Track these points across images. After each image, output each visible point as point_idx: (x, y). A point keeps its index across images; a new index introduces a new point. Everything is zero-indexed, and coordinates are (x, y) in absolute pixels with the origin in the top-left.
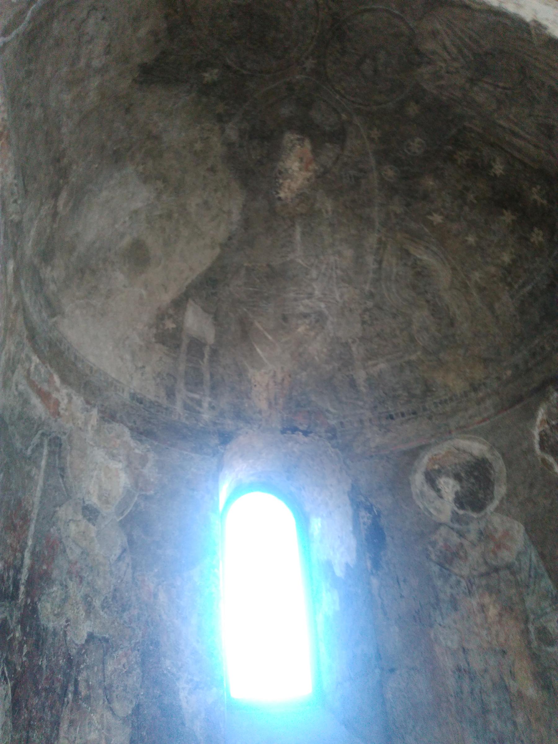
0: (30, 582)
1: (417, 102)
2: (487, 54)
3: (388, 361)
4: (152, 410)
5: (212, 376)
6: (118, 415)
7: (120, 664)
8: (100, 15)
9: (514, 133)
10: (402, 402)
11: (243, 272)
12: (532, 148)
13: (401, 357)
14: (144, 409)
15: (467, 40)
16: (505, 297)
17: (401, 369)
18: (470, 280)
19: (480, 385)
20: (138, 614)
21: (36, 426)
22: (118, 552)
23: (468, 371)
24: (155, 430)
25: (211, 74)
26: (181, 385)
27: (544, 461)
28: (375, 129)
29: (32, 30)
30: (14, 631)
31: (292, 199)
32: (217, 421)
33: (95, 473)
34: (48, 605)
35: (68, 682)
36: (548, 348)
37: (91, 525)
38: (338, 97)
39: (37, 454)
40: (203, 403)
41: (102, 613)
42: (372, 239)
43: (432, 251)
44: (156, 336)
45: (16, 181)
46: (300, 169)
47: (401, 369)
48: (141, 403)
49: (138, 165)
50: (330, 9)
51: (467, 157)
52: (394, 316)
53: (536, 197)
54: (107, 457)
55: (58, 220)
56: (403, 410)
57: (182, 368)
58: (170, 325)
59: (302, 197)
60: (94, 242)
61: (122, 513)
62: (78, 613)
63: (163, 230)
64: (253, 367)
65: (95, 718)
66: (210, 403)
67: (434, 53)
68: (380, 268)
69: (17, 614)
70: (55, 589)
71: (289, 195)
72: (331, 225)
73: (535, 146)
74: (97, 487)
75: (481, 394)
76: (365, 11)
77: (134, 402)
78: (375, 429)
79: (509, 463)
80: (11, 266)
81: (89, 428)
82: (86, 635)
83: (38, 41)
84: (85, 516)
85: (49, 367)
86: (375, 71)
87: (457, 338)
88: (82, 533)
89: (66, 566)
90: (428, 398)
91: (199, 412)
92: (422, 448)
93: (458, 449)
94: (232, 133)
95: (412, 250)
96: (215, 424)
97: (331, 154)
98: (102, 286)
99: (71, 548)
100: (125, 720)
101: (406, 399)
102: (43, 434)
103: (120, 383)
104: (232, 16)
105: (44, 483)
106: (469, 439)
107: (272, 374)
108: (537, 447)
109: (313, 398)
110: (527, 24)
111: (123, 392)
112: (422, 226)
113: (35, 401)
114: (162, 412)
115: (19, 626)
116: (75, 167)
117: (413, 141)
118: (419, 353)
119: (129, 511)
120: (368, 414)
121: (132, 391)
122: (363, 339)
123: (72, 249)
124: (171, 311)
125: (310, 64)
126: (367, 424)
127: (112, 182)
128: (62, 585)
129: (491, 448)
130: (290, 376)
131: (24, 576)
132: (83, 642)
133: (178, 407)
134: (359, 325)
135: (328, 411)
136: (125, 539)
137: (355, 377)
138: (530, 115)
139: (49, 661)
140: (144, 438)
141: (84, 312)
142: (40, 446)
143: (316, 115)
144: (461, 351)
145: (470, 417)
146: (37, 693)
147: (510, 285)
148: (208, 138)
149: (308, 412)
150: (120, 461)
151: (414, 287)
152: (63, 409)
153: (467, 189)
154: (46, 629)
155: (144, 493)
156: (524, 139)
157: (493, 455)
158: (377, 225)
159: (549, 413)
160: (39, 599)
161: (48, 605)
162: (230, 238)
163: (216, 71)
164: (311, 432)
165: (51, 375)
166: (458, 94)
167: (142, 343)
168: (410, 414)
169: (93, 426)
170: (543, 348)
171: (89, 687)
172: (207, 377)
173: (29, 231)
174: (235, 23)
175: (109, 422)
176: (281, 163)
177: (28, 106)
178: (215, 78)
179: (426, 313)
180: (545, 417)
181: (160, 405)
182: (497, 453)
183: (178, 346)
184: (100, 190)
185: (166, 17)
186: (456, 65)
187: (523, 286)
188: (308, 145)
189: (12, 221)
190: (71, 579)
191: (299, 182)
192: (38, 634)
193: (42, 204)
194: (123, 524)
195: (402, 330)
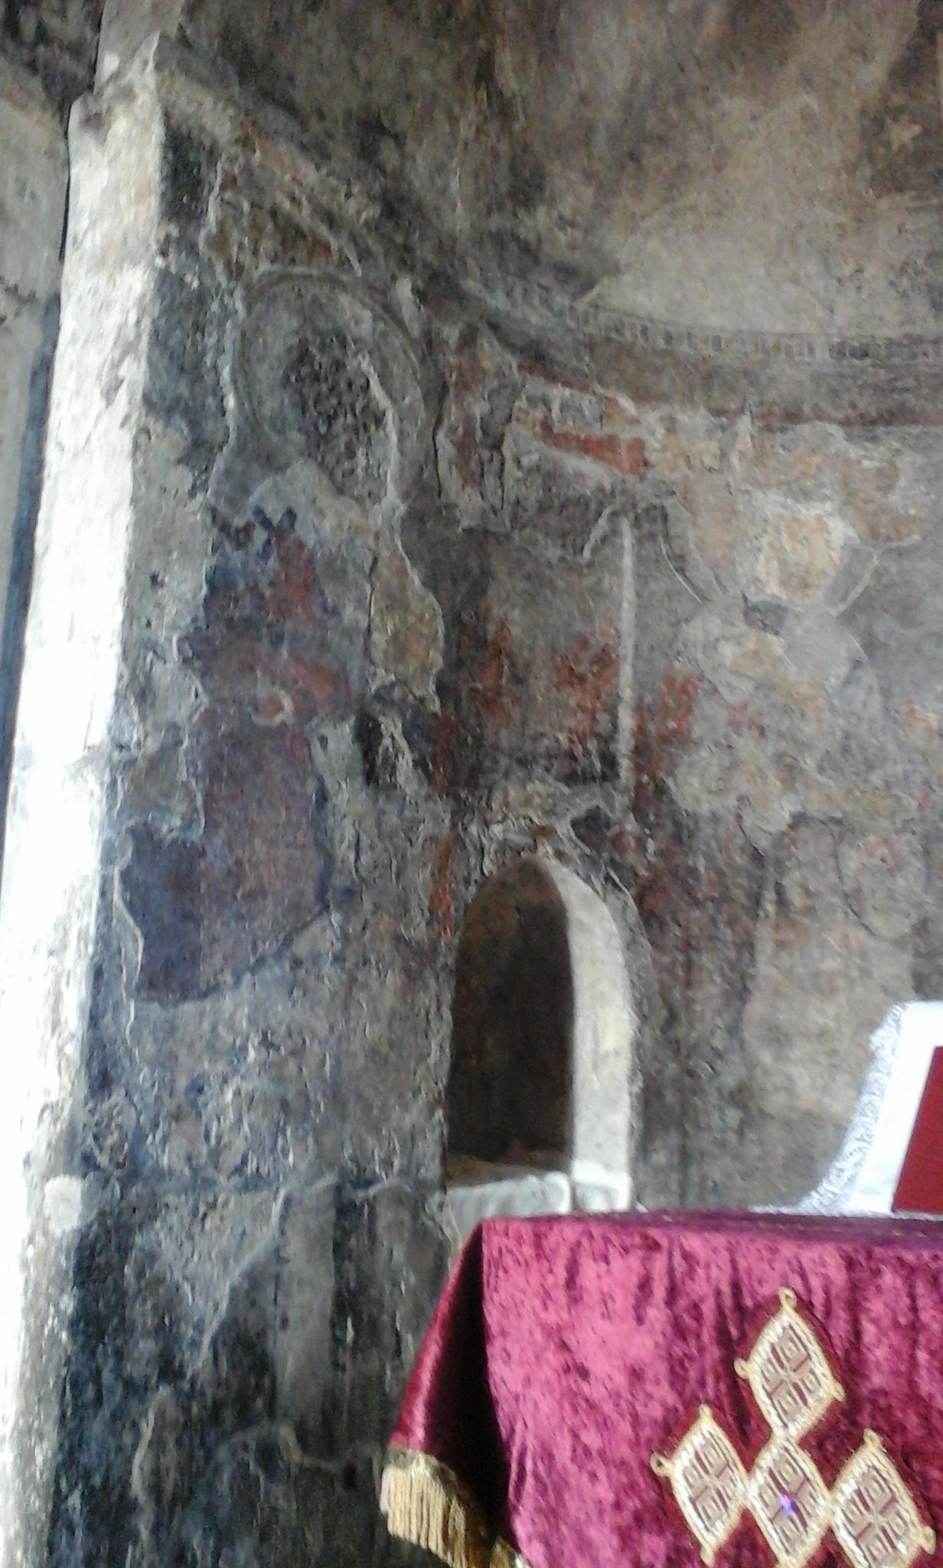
0: (640, 751)
6: (806, 409)
21: (593, 506)
22: (843, 670)
30: (620, 822)
33: (764, 541)
34: (695, 782)
35: (761, 887)
37: (771, 637)
39: (608, 551)
44: (873, 182)
45: (324, 172)
48: (865, 354)
54: (789, 501)
60: (635, 82)
61: (844, 599)
65: (833, 939)
69: (621, 801)
70: (704, 753)
74: (775, 564)
77: (845, 362)
84: (751, 623)
85: (600, 390)
89: (723, 716)
99: (729, 685)
100: (899, 943)
102: (614, 514)
105: (638, 595)
111: (811, 350)
113: (574, 463)
115: (631, 815)
121: (836, 340)
128: (717, 744)
131: (624, 745)
132: (784, 827)
136: (856, 644)
139: (710, 859)
140: (880, 430)
141: (670, 233)
142: (615, 532)
146: (697, 903)
150: (826, 498)
154: (694, 817)
155: (894, 545)
160: (670, 773)
161: (695, 782)
165: (612, 402)
167: (843, 219)
169: (742, 454)
171: (808, 893)
175: (783, 430)
181: (919, 340)
190: (738, 733)
192: (677, 824)
194: (848, 618)
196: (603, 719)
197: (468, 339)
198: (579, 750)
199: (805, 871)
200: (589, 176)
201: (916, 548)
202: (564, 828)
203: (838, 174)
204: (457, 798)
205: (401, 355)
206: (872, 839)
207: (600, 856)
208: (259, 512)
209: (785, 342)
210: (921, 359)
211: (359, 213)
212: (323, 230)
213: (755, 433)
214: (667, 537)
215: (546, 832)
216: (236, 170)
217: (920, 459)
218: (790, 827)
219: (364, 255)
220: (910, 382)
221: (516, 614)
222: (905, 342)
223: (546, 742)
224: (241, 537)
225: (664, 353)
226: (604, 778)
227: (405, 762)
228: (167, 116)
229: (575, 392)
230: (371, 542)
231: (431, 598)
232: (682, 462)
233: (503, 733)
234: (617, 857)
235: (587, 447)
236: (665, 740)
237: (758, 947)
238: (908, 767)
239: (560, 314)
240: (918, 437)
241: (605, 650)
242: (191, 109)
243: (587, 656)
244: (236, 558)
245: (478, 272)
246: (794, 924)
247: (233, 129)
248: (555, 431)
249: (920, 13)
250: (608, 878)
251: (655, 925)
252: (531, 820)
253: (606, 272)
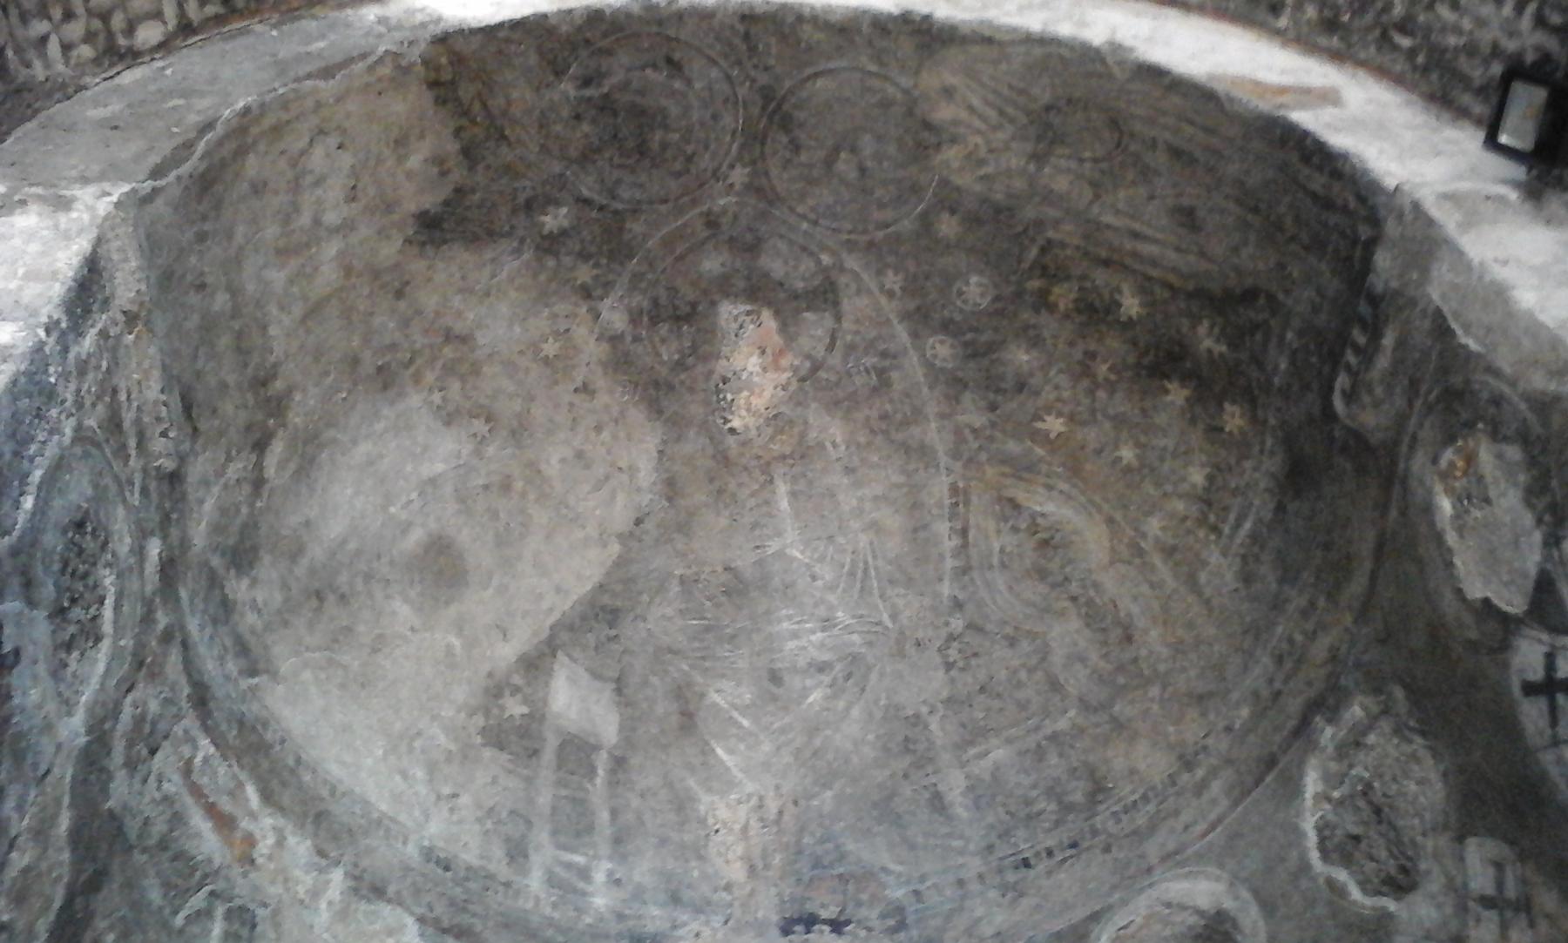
1: (953, 212)
2: (1048, 108)
3: (1009, 741)
4: (473, 885)
5: (614, 813)
8: (333, 141)
9: (1136, 235)
10: (1047, 825)
11: (675, 588)
12: (1172, 255)
13: (1037, 728)
15: (1006, 91)
16: (1214, 557)
17: (1039, 754)
18: (1144, 536)
19: (1197, 754)
21: (198, 874)
23: (1171, 729)
24: (479, 928)
25: (556, 217)
26: (542, 836)
27: (1331, 883)
28: (890, 273)
29: (208, 170)
31: (758, 428)
32: (627, 912)
36: (1299, 638)
38: (805, 226)
39: (195, 929)
42: (938, 488)
43: (1061, 492)
44: (483, 731)
45: (163, 397)
46: (765, 369)
47: (1039, 754)
48: (447, 869)
49: (431, 390)
50: (753, 81)
51: (1073, 296)
52: (1012, 642)
53: (1208, 343)
55: (265, 495)
56: (1050, 843)
57: (544, 799)
58: (515, 708)
59: (776, 421)
60: (344, 542)
63: (495, 515)
64: (709, 790)
66: (610, 874)
67: (956, 123)
68: (965, 545)
71: (751, 421)
72: (849, 470)
73: (1178, 249)
75: (1200, 773)
76: (816, 75)
78: (993, 894)
79: (1268, 907)
80: (154, 548)
81: (323, 906)
83: (219, 188)
85: (236, 768)
86: (863, 170)
87: (1144, 666)
90: (1101, 808)
91: (584, 894)
92: (1095, 917)
93: (1168, 905)
94: (615, 316)
95: (1021, 496)
96: (621, 917)
97: (819, 332)
98: (361, 628)
101: (1054, 817)
102: (212, 894)
104: (578, 117)
106: (1187, 876)
107: (754, 801)
108: (1314, 856)
109: (850, 846)
110: (1097, 51)
111: (405, 843)
112: (1029, 443)
113: (199, 822)
114: (496, 893)
116: (298, 397)
117: (967, 283)
118: (1072, 713)
120: (975, 865)
121: (426, 843)
122: (949, 701)
123: (296, 554)
124: (517, 680)
125: (739, 176)
126: (974, 887)
127: (379, 426)
129: (1232, 884)
130: (796, 803)
133: (535, 882)
134: (941, 673)
135: (884, 869)
137: (941, 788)
138: (1151, 198)
141: (323, 676)
142: (204, 914)
143: (774, 264)
144: (1154, 691)
145: (1186, 828)
147: (1215, 529)
148: (567, 330)
149: (840, 876)
151: (1042, 574)
152: (262, 855)
153: (1092, 356)
156: (1156, 241)
157: (1236, 898)
158: (944, 460)
159: (1327, 778)
162: (638, 522)
163: (564, 210)
164: (848, 922)
165: (240, 785)
166: (1019, 184)
167: (453, 747)
168: (1063, 850)
169: (330, 903)
170: (1291, 641)
172: (605, 816)
173: (201, 502)
174: (586, 127)
175: (369, 901)
176: (723, 362)
177: (202, 287)
178: (566, 223)
179: (1075, 623)
180: (1320, 788)
181: (490, 877)
182: (1245, 894)
183: (535, 753)
184: (355, 442)
185: (458, 132)
186: (1001, 135)
187: (1238, 525)
188: (768, 320)
189: (158, 468)
191: (767, 394)
193: (229, 459)
195: (1031, 671)
200: (285, 587)
203: (459, 711)
211: (160, 456)
212: (132, 443)
219: (145, 491)
228: (99, 241)
229: (218, 754)
231: (66, 856)
235: (212, 810)
239: (227, 678)
242: (115, 257)
247: (132, 301)
249: (551, 628)
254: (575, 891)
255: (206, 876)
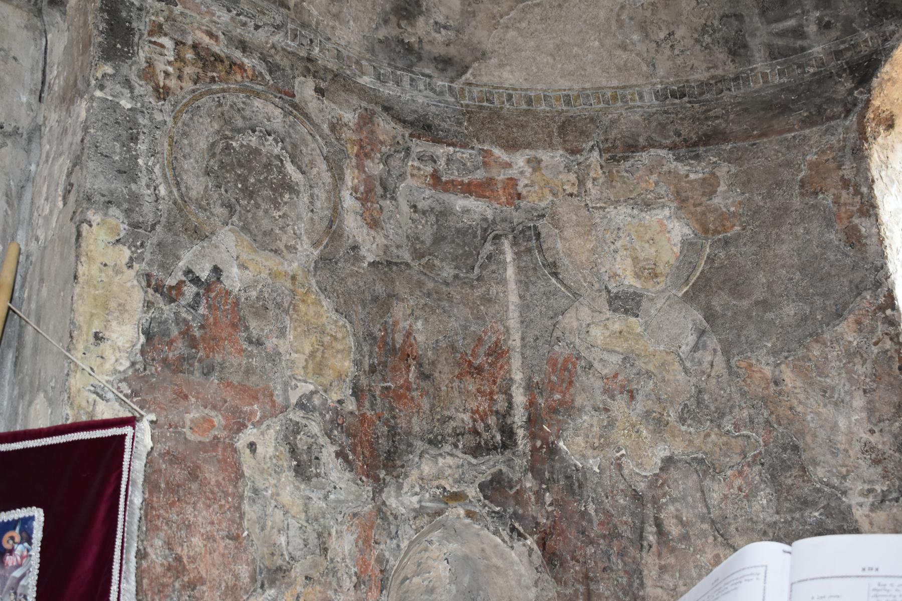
0: (532, 421)
4: (707, 96)
6: (642, 141)
7: (733, 487)
14: (690, 102)
20: (750, 416)
22: (691, 339)
30: (520, 481)
33: (619, 244)
35: (643, 522)
37: (633, 319)
40: (805, 29)
41: (684, 428)
48: (683, 95)
54: (635, 212)
61: (687, 280)
62: (639, 436)
69: (521, 463)
74: (629, 261)
77: (668, 102)
82: (659, 462)
88: (618, 334)
89: (599, 384)
91: (803, 49)
103: (631, 87)
111: (641, 97)
113: (460, 203)
114: (730, 90)
115: (530, 475)
119: (698, 274)
128: (596, 409)
131: (519, 417)
133: (760, 63)
136: (700, 317)
139: (598, 502)
140: (701, 150)
141: (524, 24)
155: (720, 236)
165: (487, 153)
169: (594, 179)
175: (626, 159)
181: (722, 80)
196: (500, 398)
197: (366, 120)
198: (480, 426)
199: (678, 505)
201: (739, 236)
202: (472, 492)
204: (377, 479)
205: (309, 138)
206: (729, 473)
207: (505, 511)
208: (188, 272)
209: (620, 92)
210: (726, 92)
212: (237, 54)
213: (603, 164)
214: (541, 250)
215: (457, 497)
216: (162, 19)
217: (734, 169)
218: (661, 469)
220: (719, 111)
221: (419, 325)
222: (712, 82)
223: (453, 424)
224: (172, 294)
225: (527, 112)
226: (505, 446)
227: (328, 453)
230: (289, 284)
232: (546, 191)
233: (415, 420)
234: (520, 511)
235: (468, 189)
236: (554, 410)
237: (645, 572)
238: (752, 411)
239: (441, 93)
240: (731, 152)
241: (496, 343)
243: (482, 350)
244: (168, 310)
245: (371, 70)
246: (673, 550)
248: (444, 179)
250: (513, 529)
251: (557, 563)
252: (445, 489)
253: (476, 59)
254: (795, 51)
255: (485, 230)
